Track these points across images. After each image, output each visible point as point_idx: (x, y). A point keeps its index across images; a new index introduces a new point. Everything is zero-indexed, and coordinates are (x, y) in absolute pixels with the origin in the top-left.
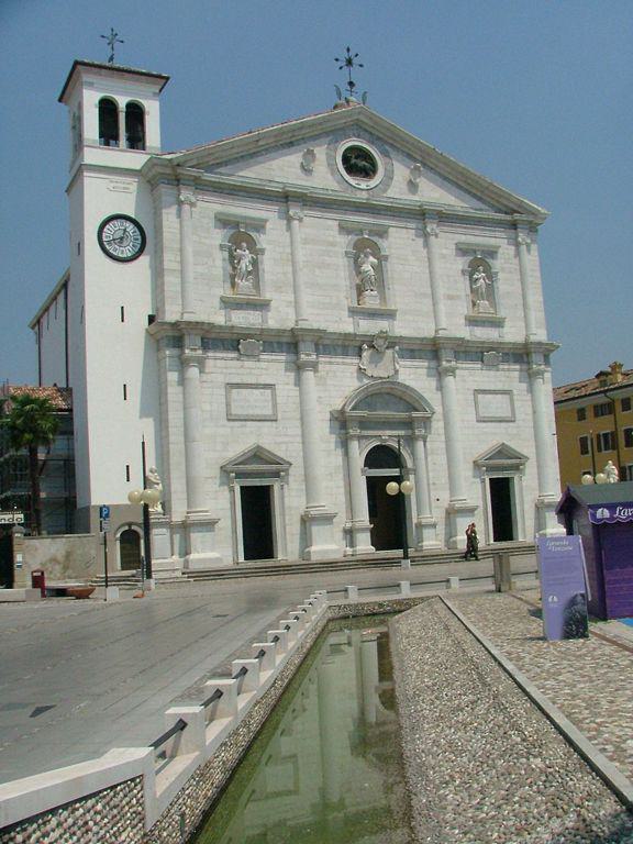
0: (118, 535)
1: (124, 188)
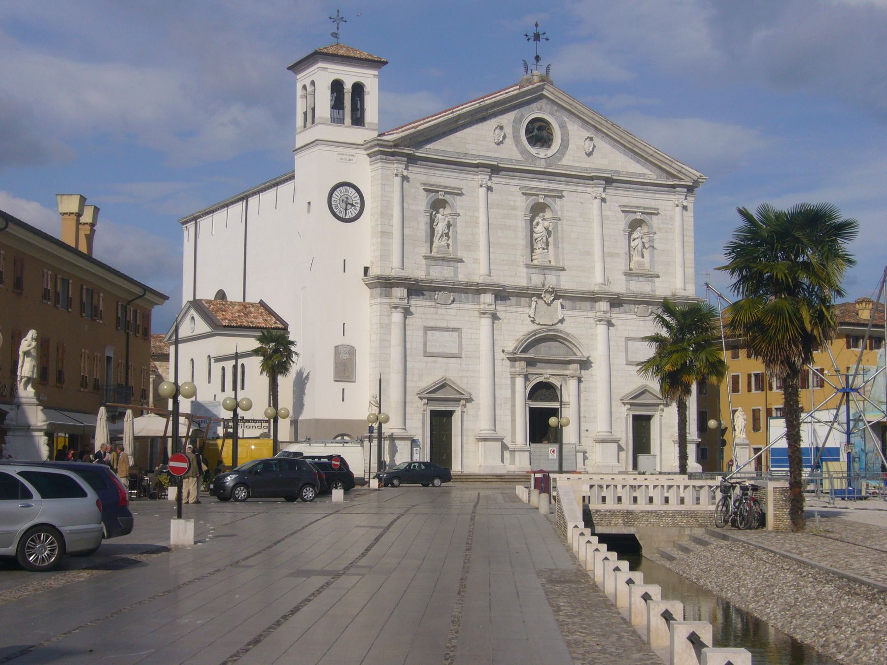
1: (349, 160)
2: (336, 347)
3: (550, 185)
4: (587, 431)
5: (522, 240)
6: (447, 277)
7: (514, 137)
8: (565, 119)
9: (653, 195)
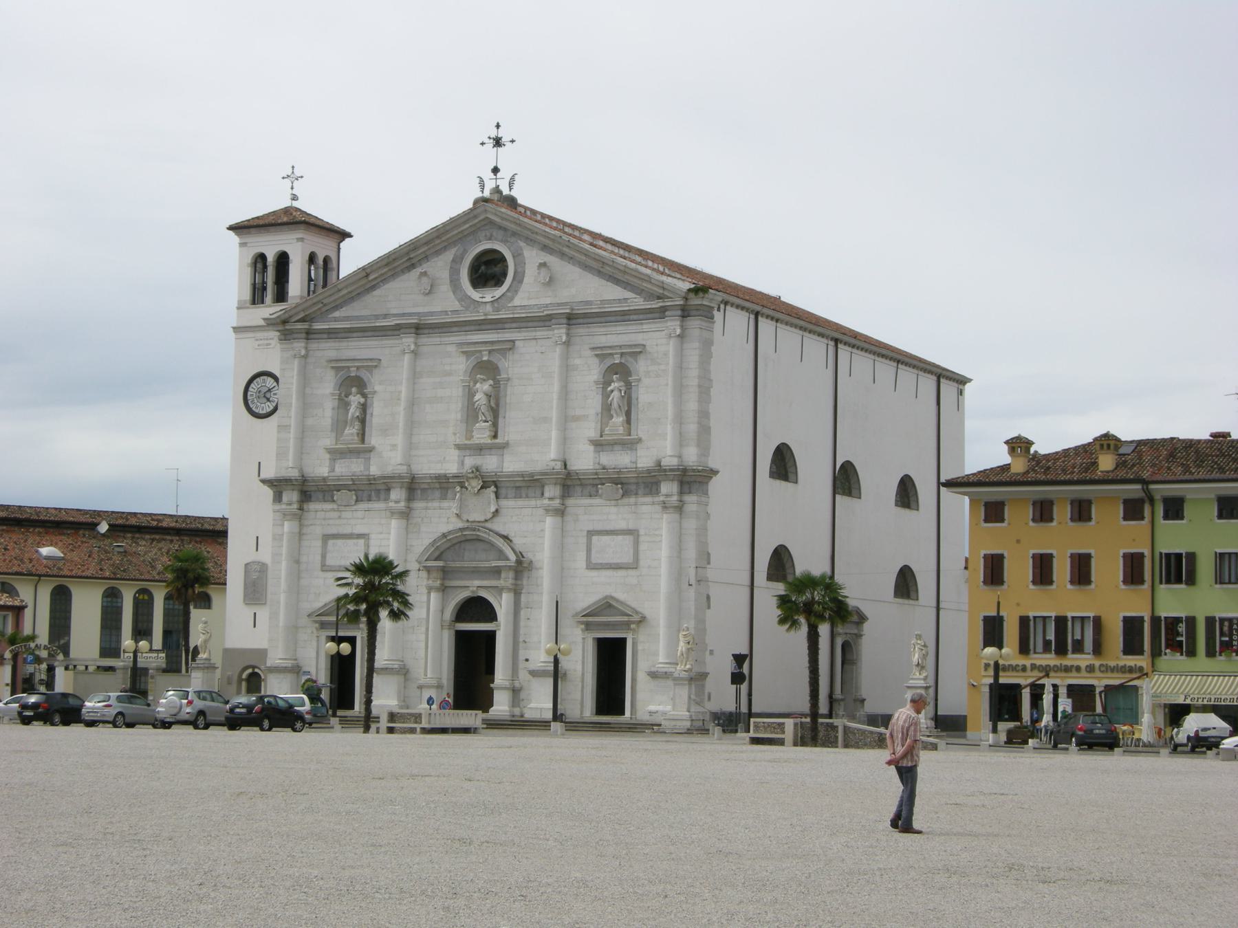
0: (244, 676)
2: (246, 565)
3: (500, 335)
4: (527, 660)
5: (454, 412)
6: (355, 472)
7: (451, 281)
8: (522, 244)
9: (639, 327)
